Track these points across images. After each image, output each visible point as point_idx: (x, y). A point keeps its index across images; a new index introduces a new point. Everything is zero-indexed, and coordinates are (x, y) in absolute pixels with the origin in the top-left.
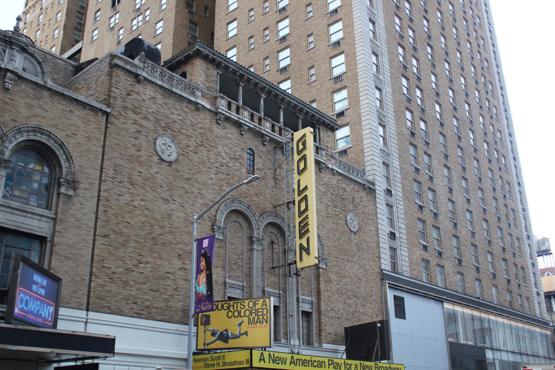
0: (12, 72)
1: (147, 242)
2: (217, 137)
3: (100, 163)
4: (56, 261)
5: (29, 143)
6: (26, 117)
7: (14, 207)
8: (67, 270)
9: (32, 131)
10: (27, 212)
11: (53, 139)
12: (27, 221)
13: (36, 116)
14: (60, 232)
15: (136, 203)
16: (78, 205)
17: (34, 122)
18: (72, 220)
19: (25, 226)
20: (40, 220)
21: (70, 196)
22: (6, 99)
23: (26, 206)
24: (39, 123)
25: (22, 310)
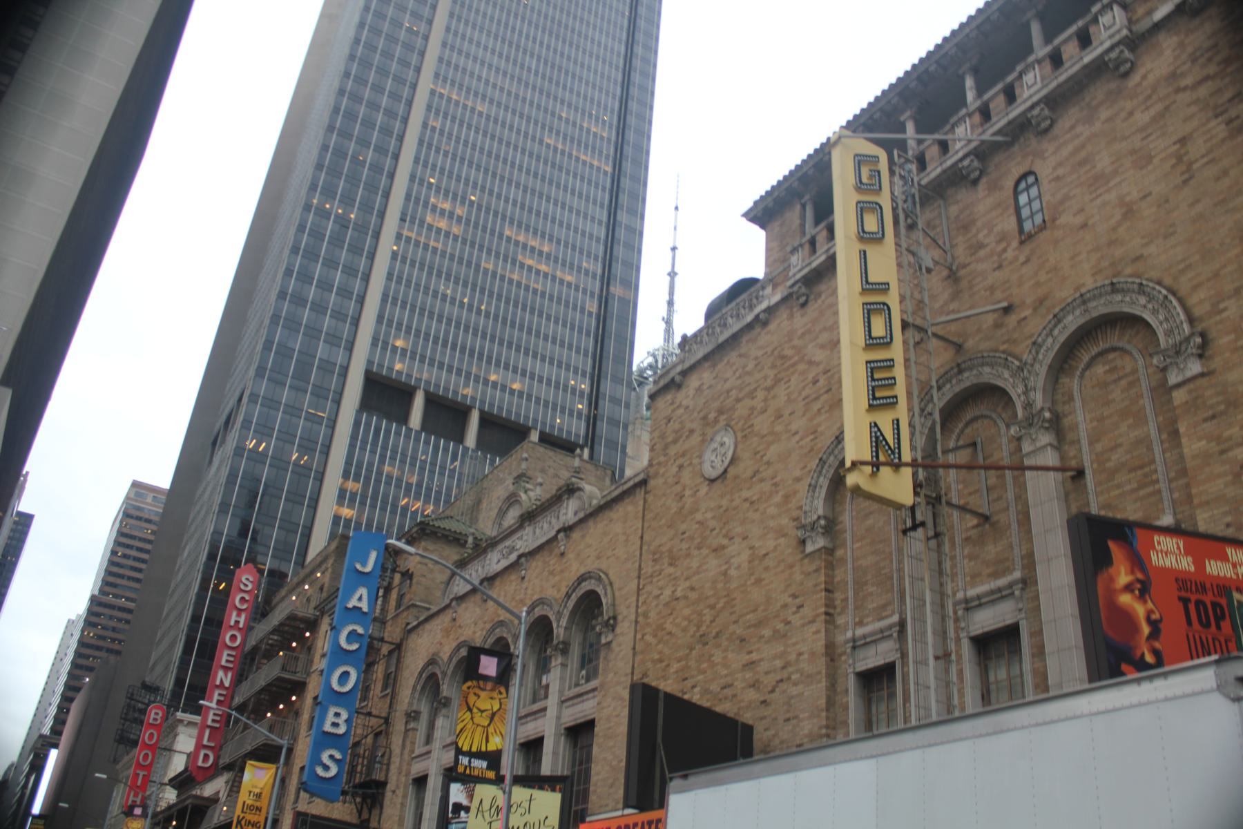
0: (559, 532)
1: (692, 649)
2: (803, 334)
3: (637, 565)
15: (679, 594)
17: (582, 571)
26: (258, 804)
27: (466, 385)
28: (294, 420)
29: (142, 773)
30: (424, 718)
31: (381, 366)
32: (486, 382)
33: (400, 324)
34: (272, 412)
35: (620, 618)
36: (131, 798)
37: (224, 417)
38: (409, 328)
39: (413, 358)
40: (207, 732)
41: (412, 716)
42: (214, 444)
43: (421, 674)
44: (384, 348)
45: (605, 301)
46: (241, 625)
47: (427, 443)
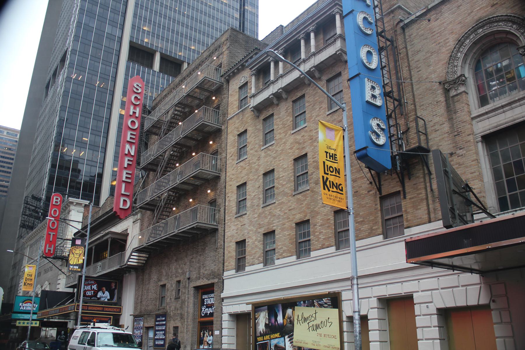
26: (335, 165)
27: (180, 51)
28: (96, 64)
29: (52, 234)
31: (137, 39)
32: (190, 49)
33: (145, 19)
34: (84, 59)
36: (47, 248)
37: (52, 72)
38: (150, 21)
39: (153, 36)
40: (124, 185)
41: (450, 86)
42: (47, 87)
43: (460, 43)
44: (138, 31)
45: (243, 13)
46: (137, 115)
47: (163, 78)
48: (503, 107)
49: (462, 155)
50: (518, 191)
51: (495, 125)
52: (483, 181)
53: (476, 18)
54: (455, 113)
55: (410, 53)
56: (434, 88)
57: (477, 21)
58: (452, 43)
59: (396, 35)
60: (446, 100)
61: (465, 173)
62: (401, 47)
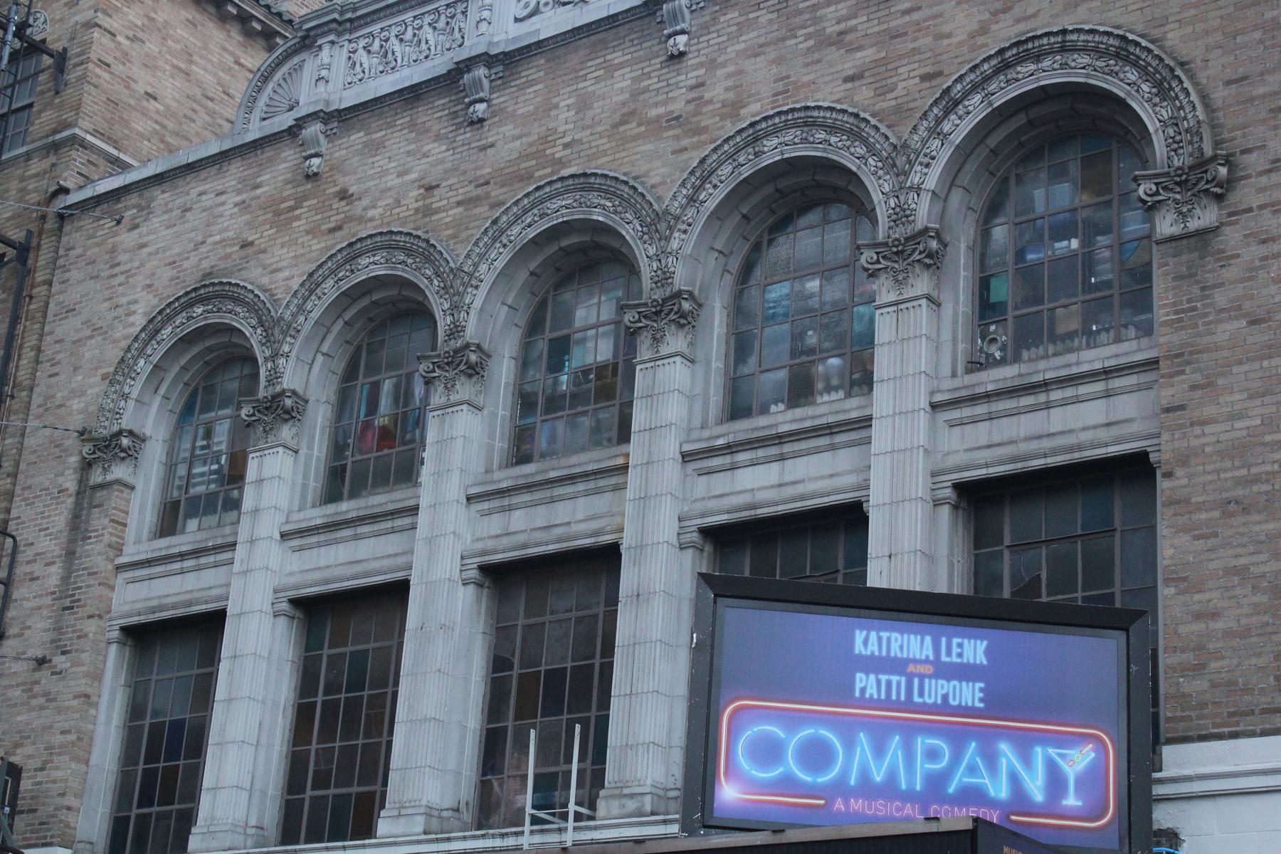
4: (1184, 539)
5: (1021, 120)
6: (972, 36)
7: (990, 387)
8: (1242, 561)
9: (997, 71)
10: (1045, 385)
11: (1084, 50)
12: (1058, 419)
13: (1005, 11)
14: (1182, 407)
16: (1258, 251)
17: (1006, 32)
18: (1227, 329)
19: (1047, 444)
20: (1108, 395)
21: (1204, 234)
22: (893, 24)
23: (1042, 365)
24: (1022, 27)
25: (787, 784)
30: (154, 454)
35: (1254, 161)
43: (152, 328)
48: (182, 556)
49: (60, 673)
50: (155, 809)
51: (154, 603)
52: (87, 762)
53: (205, 264)
54: (85, 538)
55: (52, 307)
56: (68, 443)
57: (208, 275)
58: (139, 320)
59: (40, 234)
60: (78, 493)
61: (51, 727)
62: (40, 276)
